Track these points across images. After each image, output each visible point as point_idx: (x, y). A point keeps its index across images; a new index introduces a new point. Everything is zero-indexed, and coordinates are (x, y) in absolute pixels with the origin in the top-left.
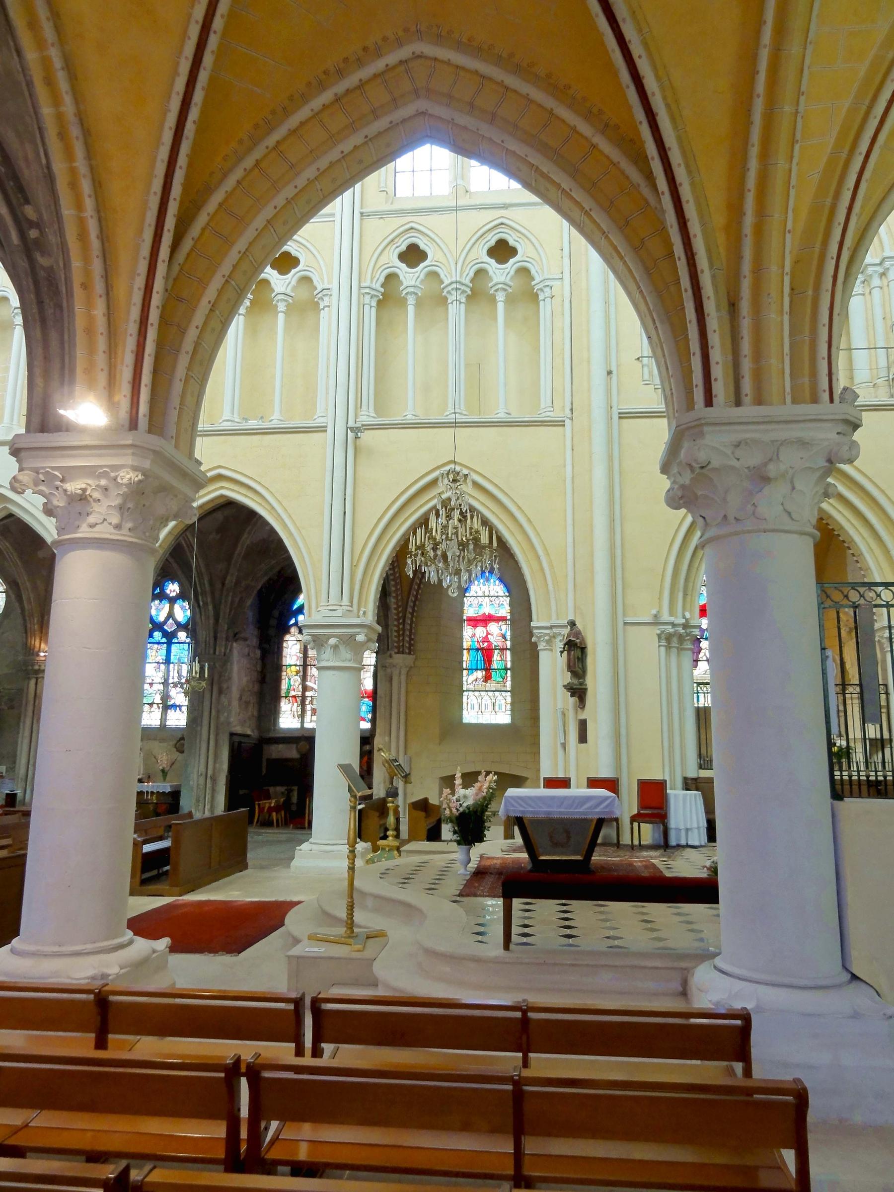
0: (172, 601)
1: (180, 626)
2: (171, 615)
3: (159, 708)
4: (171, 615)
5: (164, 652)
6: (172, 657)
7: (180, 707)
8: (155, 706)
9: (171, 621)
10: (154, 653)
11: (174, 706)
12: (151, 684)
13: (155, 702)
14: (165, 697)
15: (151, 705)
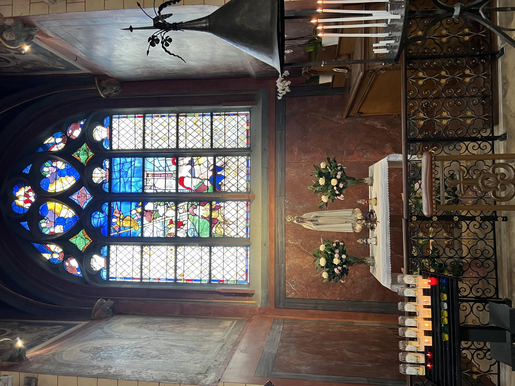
0: (43, 197)
1: (84, 180)
2: (64, 198)
4: (64, 198)
6: (134, 190)
7: (216, 169)
8: (214, 215)
10: (126, 224)
11: (216, 179)
12: (179, 224)
13: (206, 214)
14: (197, 198)
15: (212, 222)
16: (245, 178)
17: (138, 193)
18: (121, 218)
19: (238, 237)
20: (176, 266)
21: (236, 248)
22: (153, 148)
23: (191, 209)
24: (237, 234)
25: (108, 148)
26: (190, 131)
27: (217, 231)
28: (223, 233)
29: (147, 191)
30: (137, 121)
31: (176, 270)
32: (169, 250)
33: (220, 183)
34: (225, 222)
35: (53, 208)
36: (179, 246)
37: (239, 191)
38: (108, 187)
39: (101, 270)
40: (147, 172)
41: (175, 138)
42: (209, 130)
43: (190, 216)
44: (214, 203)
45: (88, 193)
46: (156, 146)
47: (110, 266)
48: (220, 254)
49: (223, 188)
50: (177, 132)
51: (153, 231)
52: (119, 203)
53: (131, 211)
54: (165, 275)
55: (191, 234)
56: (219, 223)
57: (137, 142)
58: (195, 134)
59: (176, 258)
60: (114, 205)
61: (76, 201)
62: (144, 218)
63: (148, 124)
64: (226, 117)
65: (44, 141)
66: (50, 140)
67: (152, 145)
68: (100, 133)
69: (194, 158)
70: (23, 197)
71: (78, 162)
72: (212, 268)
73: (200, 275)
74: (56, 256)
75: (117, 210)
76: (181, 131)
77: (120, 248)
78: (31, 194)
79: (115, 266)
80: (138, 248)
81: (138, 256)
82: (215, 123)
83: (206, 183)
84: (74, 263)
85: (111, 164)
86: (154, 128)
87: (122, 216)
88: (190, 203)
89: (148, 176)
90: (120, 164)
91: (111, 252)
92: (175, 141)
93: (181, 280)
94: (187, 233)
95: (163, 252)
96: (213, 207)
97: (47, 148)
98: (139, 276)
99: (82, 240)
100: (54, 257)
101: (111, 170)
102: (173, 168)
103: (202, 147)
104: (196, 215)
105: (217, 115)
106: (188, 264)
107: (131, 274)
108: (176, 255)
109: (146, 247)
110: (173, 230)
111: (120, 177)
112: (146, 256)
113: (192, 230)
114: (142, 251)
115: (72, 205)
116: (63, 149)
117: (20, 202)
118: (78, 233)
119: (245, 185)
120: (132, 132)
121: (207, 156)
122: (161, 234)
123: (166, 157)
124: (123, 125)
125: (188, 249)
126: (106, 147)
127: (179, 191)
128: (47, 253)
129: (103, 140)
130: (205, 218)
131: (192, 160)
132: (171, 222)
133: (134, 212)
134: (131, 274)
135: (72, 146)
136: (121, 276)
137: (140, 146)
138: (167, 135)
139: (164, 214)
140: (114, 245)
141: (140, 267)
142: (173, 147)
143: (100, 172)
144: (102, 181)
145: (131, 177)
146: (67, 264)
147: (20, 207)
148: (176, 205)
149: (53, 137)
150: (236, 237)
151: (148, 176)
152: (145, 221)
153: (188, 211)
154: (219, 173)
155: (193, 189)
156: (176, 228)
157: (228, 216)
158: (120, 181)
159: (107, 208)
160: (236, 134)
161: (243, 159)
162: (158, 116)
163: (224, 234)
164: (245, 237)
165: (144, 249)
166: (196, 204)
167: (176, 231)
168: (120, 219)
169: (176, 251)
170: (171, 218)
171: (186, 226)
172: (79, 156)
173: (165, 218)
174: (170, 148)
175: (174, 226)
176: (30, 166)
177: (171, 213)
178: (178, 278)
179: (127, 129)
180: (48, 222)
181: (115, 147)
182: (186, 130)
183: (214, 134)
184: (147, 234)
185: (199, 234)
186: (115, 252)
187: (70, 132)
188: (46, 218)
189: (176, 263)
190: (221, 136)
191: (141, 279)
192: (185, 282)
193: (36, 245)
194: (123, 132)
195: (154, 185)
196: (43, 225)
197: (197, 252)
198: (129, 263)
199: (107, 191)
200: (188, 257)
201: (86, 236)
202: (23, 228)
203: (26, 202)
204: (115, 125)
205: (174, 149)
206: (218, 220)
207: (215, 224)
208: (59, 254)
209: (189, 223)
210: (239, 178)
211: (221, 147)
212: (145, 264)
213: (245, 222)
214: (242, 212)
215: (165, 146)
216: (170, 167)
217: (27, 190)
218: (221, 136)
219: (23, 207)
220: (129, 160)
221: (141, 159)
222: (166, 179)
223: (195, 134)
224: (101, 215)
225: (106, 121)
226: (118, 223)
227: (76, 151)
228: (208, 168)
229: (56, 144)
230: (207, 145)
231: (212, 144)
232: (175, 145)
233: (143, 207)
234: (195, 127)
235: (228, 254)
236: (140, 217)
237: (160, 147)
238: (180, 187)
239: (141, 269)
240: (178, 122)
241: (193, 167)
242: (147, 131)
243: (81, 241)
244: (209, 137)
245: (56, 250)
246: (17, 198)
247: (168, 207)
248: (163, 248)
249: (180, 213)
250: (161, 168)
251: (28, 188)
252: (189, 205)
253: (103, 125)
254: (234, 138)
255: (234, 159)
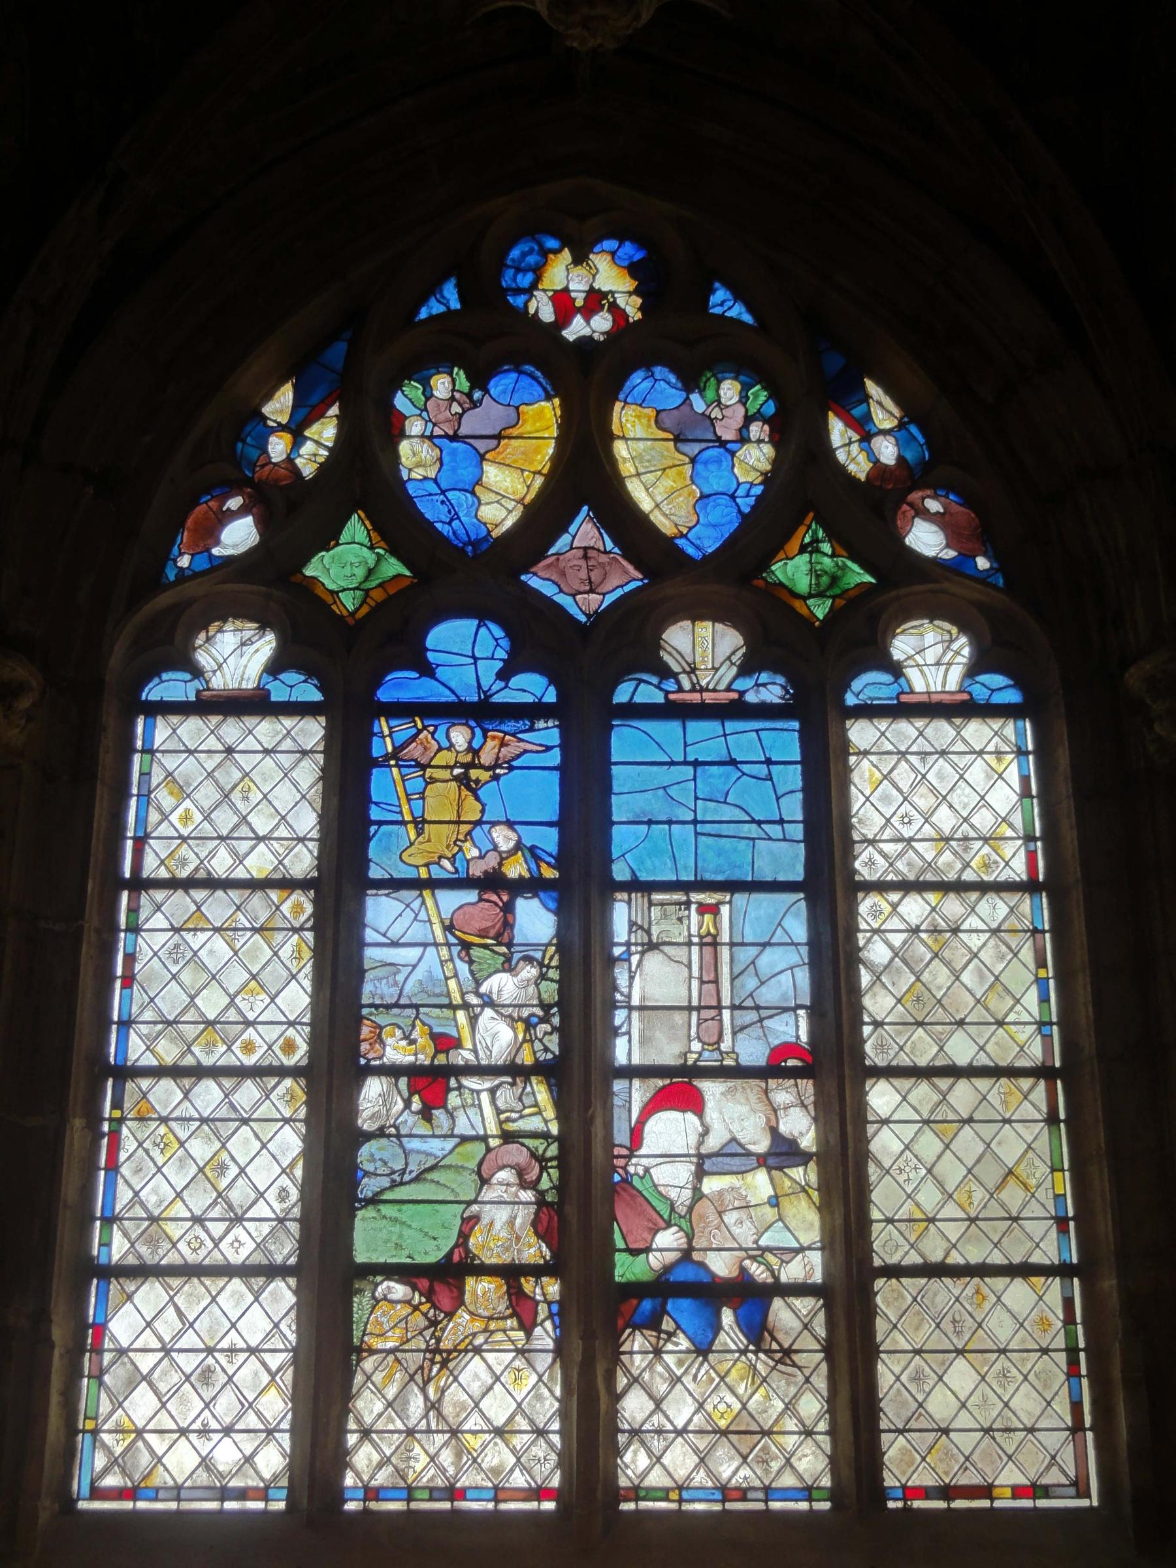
0: (587, 381)
2: (583, 477)
3: (522, 1311)
4: (583, 477)
5: (533, 791)
7: (751, 1297)
8: (483, 1290)
9: (584, 530)
10: (442, 799)
12: (431, 1083)
13: (490, 1245)
14: (583, 1194)
15: (442, 1279)
16: (700, 1478)
17: (607, 860)
18: (474, 773)
19: (352, 1439)
20: (199, 1072)
21: (285, 1425)
22: (861, 939)
23: (516, 1153)
24: (366, 1433)
25: (850, 700)
26: (968, 1142)
27: (386, 1314)
28: (379, 1344)
29: (621, 915)
30: (1008, 849)
31: (175, 1072)
32: (291, 1032)
33: (667, 1324)
34: (443, 1358)
35: (526, 428)
36: (310, 1092)
37: (622, 1439)
38: (638, 699)
39: (197, 672)
40: (725, 910)
41: (922, 1062)
42: (974, 1255)
43: (478, 1149)
44: (553, 1288)
45: (610, 599)
46: (877, 953)
47: (214, 720)
48: (255, 1327)
49: (638, 1342)
50: (954, 1072)
51: (395, 944)
52: (555, 758)
53: (510, 824)
54: (148, 1015)
55: (372, 1159)
56: (434, 1323)
57: (890, 848)
58: (952, 1172)
59: (241, 1073)
60: (548, 733)
61: (565, 539)
62: (471, 896)
63: (995, 909)
64: (1061, 1358)
65: (879, 382)
66: (884, 411)
67: (876, 931)
68: (931, 654)
69: (812, 1165)
70: (587, 285)
71: (774, 549)
72: (175, 1282)
73: (139, 1212)
74: (278, 447)
75: (514, 748)
76: (963, 1094)
77: (308, 773)
78: (602, 323)
79: (213, 743)
80: (303, 862)
81: (259, 863)
82: (1018, 1293)
83: (669, 1239)
84: (239, 535)
85: (764, 711)
86: (975, 941)
87: (484, 775)
88: (553, 1150)
89: (703, 909)
90: (769, 762)
91: (288, 722)
92: (904, 1060)
93: (117, 1104)
94: (381, 1133)
95: (284, 1005)
96: (528, 1285)
97: (846, 397)
98: (151, 867)
99: (360, 573)
100: (273, 439)
101: (737, 710)
102: (753, 1052)
103: (875, 1214)
104: (484, 1181)
105: (1068, 1303)
106: (201, 1149)
107: (164, 830)
108: (257, 1072)
109: (309, 908)
110: (396, 1052)
111: (696, 764)
112: (259, 905)
113: (399, 1166)
114: (287, 884)
115: (544, 519)
116: (841, 470)
117: (561, 273)
118: (394, 551)
119: (656, 1479)
120: (945, 820)
121: (827, 1246)
122: (373, 989)
123: (816, 1012)
124: (977, 773)
125: (290, 1142)
126: (857, 685)
127: (618, 1085)
128: (296, 406)
129: (896, 670)
130: (464, 1236)
131: (802, 1158)
132: (444, 1043)
133: (504, 838)
134: (164, 830)
135: (865, 515)
136: (157, 776)
137: (868, 864)
138: (940, 1014)
139: (489, 1002)
140: (328, 738)
141: (202, 874)
142: (868, 1048)
143: (720, 658)
144: (676, 668)
145: (695, 822)
146: (234, 503)
147: (538, 272)
148: (539, 1069)
149: (901, 425)
150: (352, 1425)
151: (703, 909)
152: (451, 900)
153: (508, 1137)
154: (727, 1317)
155: (636, 1167)
156: (413, 1072)
157: (473, 1372)
158: (672, 763)
159: (529, 699)
160: (964, 1420)
161: (812, 1462)
162: (1041, 963)
163: (372, 1352)
164: (349, 1480)
165: (298, 896)
166: (545, 1184)
167: (393, 1071)
168: (467, 766)
169: (281, 1072)
170: (468, 1044)
171: (423, 1129)
172: (803, 549)
173: (466, 1006)
174: (867, 1030)
175: (424, 1060)
176: (747, 318)
177: (496, 1038)
178: (130, 1085)
179: (963, 798)
180: (456, 408)
181: (860, 733)
182: (970, 1120)
183: (953, 1286)
184: (383, 913)
185: (374, 1201)
186: (288, 744)
187: (934, 506)
188: (477, 395)
189: (215, 1072)
190: (946, 1325)
191: (139, 884)
192: (106, 1127)
193: (337, 352)
194: (940, 772)
195: (651, 946)
196: (441, 385)
197: (271, 1195)
198: (225, 820)
199: (622, 694)
200: (242, 1143)
201: (378, 596)
202: (432, 289)
203: (562, 299)
204: (977, 731)
205: (862, 1055)
206: (450, 1315)
207: (429, 1295)
208: (290, 460)
209: (437, 1147)
210: (702, 1443)
211: (881, 1325)
212: (218, 906)
213: (440, 1482)
214: (498, 1455)
215: (878, 1003)
216: (756, 1031)
217: (621, 301)
218: (946, 1325)
219: (534, 286)
220: (794, 807)
221: (797, 873)
222: (690, 1008)
223: (952, 1172)
224: (488, 671)
225: (997, 687)
226: (444, 758)
227: (831, 536)
228: (760, 1253)
229: (866, 437)
230: (888, 1245)
231: (895, 1272)
232: (881, 1061)
233: (532, 886)
234: (991, 1174)
235: (249, 1373)
236: (477, 870)
237: (865, 978)
238: (639, 1093)
239: (188, 884)
240: (1012, 1072)
241: (762, 1161)
242: (953, 906)
243: (348, 565)
244: (936, 1256)
245: (308, 448)
246: (579, 259)
247: (529, 1025)
248: (297, 998)
249: (493, 1092)
250: (751, 983)
251: (632, 307)
252: (539, 1145)
253: (974, 670)
254: (940, 1405)
255: (811, 1406)
